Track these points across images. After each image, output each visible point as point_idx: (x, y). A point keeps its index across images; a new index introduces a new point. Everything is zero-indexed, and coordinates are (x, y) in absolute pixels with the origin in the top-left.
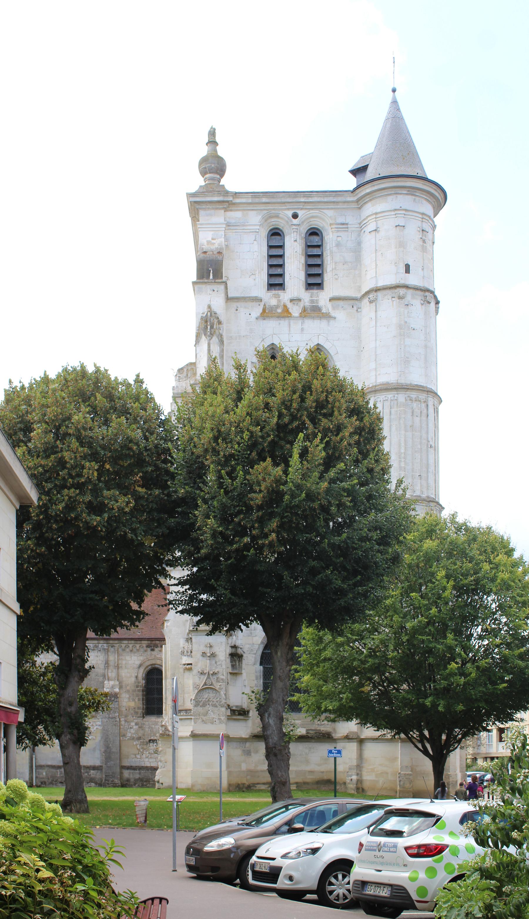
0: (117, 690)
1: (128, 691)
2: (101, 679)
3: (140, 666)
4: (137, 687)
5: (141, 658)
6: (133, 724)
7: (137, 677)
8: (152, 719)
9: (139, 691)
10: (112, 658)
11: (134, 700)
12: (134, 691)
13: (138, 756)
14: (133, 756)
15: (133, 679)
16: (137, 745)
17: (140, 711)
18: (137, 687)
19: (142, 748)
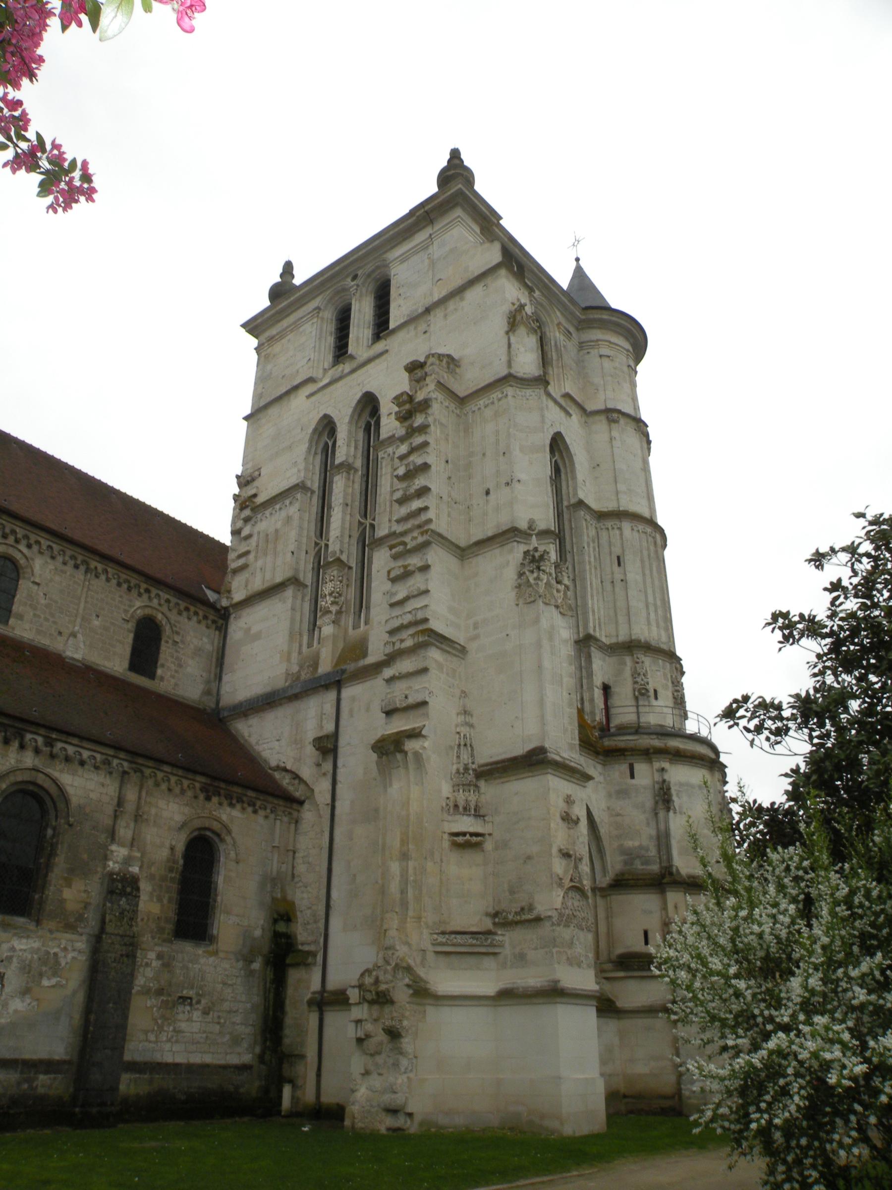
0: (135, 869)
1: (151, 877)
2: (103, 838)
3: (184, 825)
4: (171, 870)
5: (187, 810)
6: (152, 955)
7: (172, 849)
8: (188, 948)
9: (172, 879)
10: (131, 795)
11: (160, 900)
12: (163, 879)
13: (152, 1037)
14: (142, 1037)
15: (165, 853)
16: (152, 1007)
17: (170, 927)
18: (171, 870)
19: (163, 1017)
